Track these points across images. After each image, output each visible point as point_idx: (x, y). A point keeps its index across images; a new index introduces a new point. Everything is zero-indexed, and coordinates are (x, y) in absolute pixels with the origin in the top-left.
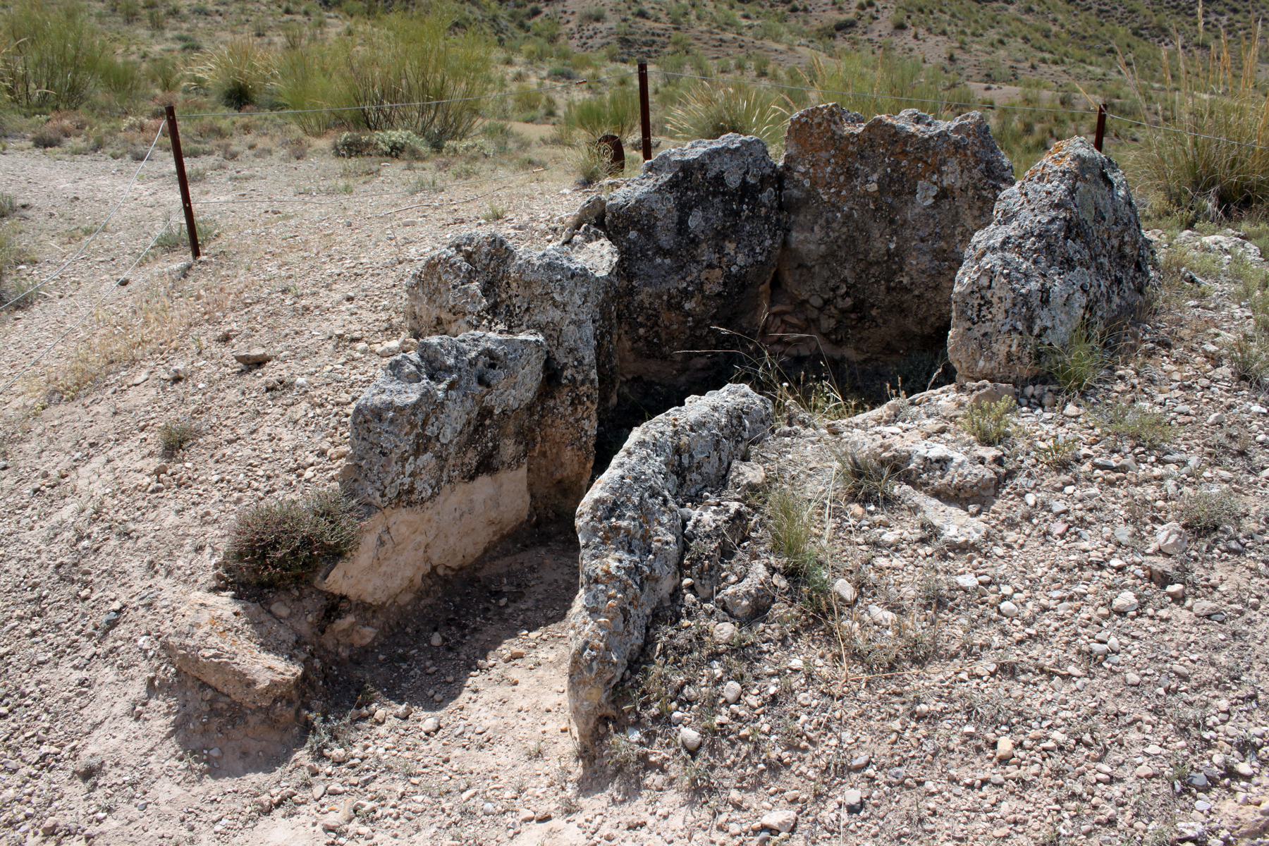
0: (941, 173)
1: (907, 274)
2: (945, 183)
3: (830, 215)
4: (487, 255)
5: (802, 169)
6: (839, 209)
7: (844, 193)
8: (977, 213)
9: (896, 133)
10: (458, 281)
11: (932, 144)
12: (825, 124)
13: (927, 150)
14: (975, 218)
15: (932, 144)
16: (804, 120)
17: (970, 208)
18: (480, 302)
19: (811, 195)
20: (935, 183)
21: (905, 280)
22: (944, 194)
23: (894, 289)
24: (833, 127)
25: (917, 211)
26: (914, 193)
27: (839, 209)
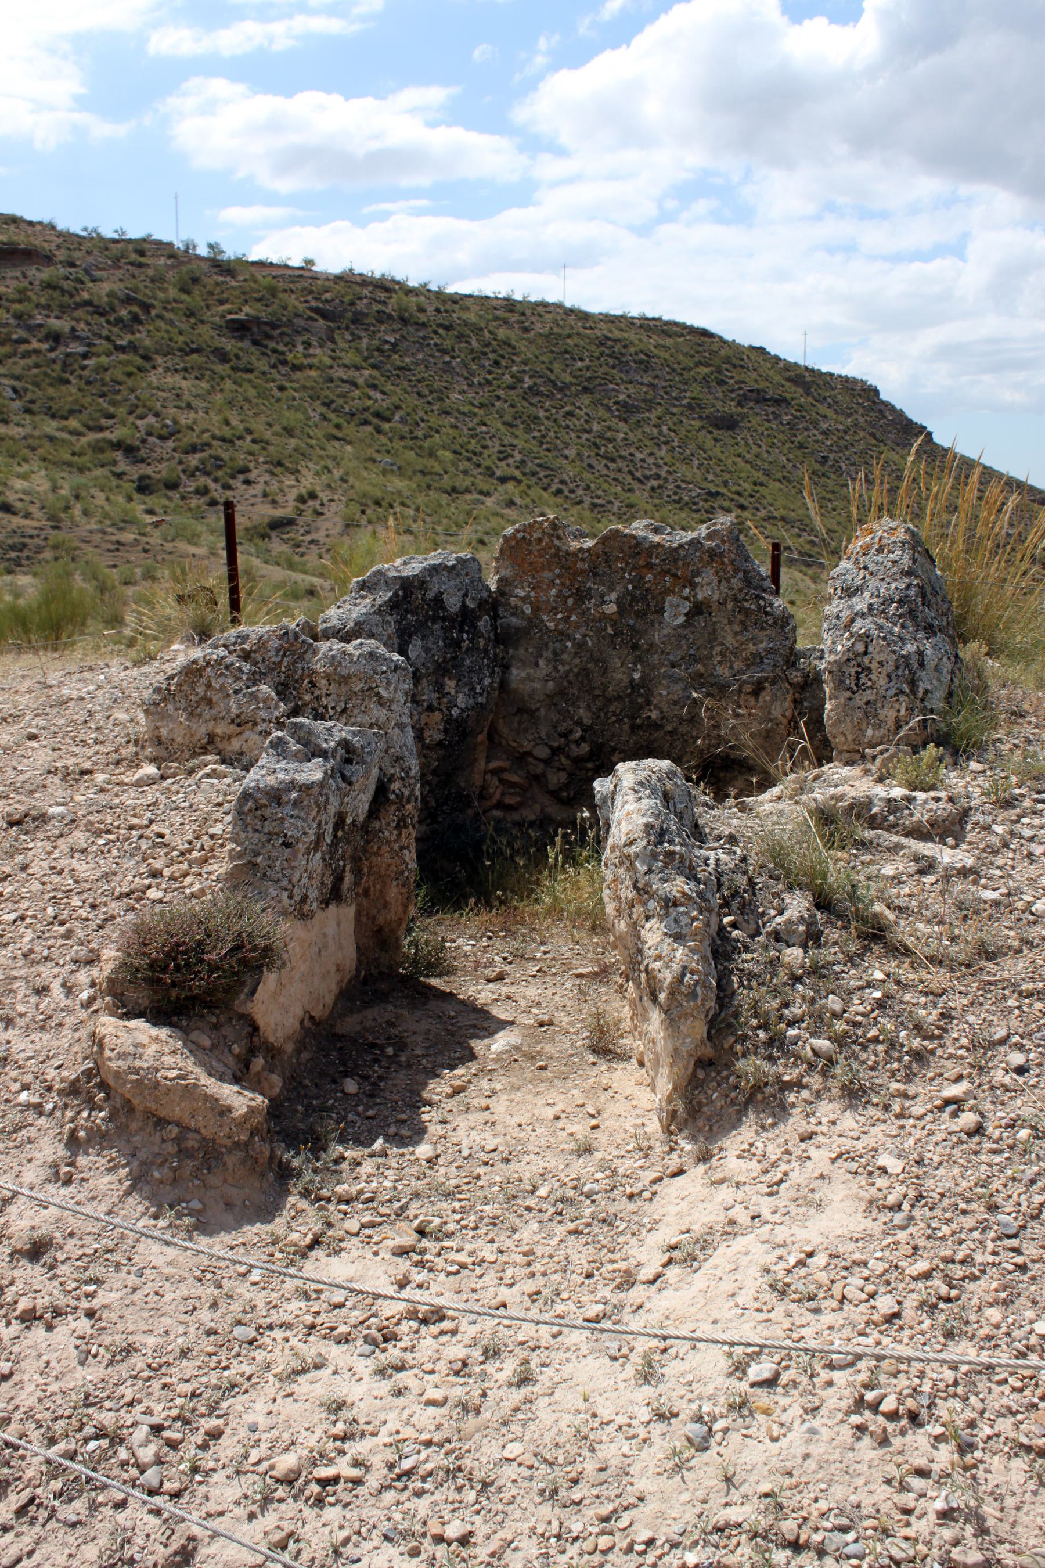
0: (693, 586)
1: (656, 707)
2: (700, 597)
3: (557, 645)
4: (278, 651)
5: (522, 594)
6: (569, 637)
7: (574, 618)
8: (737, 628)
9: (638, 544)
10: (239, 685)
11: (682, 553)
12: (546, 539)
13: (676, 561)
15: (682, 553)
16: (520, 535)
17: (730, 623)
18: (277, 707)
19: (534, 622)
20: (687, 599)
21: (654, 715)
22: (698, 609)
23: (640, 727)
24: (556, 542)
26: (661, 611)
27: (569, 637)
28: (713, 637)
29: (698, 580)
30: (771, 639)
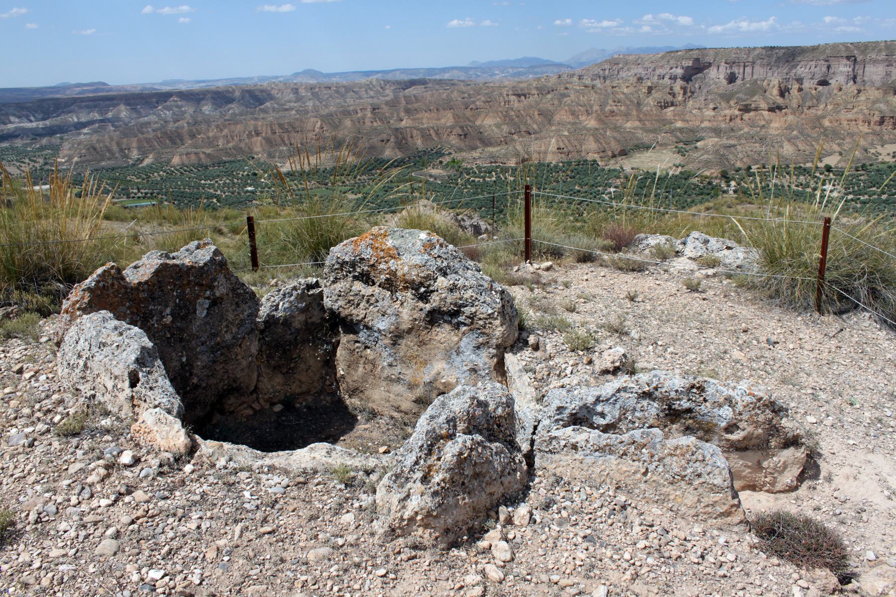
2: (218, 294)
11: (206, 268)
14: (233, 311)
15: (206, 268)
16: (101, 284)
17: (232, 304)
20: (208, 298)
21: (195, 381)
22: (215, 302)
25: (198, 324)
26: (195, 312)
28: (222, 317)
29: (216, 284)
30: (250, 308)
